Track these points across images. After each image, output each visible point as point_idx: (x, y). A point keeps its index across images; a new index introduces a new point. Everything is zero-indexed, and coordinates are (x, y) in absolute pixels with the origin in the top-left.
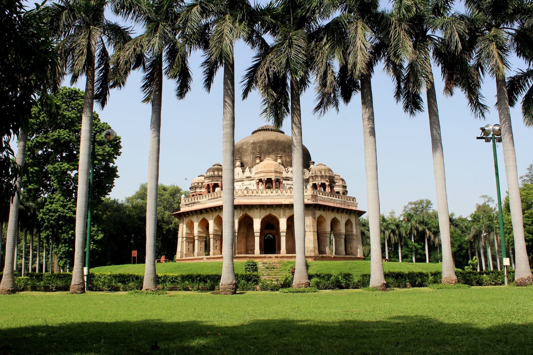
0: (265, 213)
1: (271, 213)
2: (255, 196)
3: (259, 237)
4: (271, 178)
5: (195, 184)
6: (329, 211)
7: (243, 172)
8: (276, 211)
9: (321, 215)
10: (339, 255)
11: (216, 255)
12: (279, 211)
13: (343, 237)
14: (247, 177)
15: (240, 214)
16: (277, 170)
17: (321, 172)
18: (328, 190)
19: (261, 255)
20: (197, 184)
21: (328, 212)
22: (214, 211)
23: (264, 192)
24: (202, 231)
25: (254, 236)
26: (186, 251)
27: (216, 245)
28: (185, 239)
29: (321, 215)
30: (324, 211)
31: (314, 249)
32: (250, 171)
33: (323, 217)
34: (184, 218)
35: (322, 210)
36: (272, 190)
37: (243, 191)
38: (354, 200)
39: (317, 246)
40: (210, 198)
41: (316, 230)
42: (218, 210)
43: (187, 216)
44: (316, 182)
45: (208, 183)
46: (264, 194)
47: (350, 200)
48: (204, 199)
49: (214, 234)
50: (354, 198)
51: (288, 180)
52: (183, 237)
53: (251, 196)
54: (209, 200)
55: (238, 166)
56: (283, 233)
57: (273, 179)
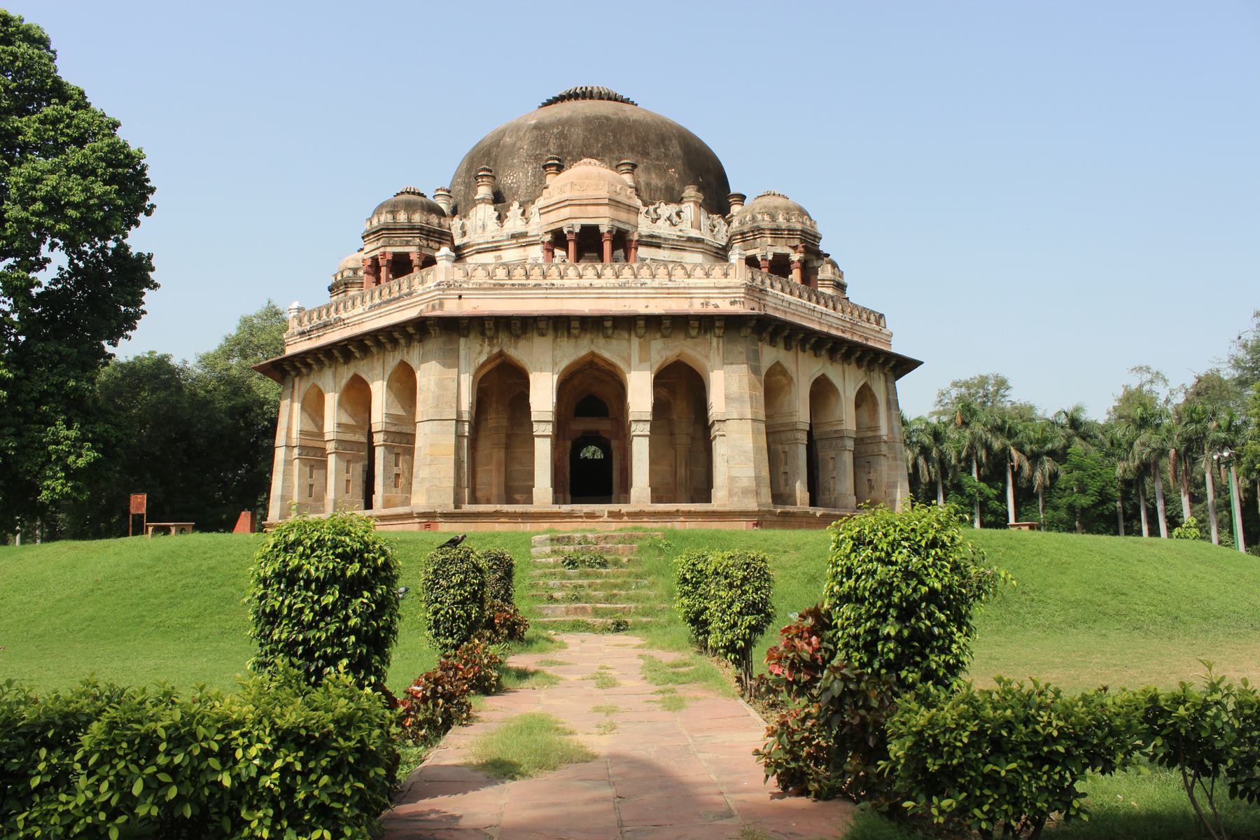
0: (572, 351)
1: (596, 351)
2: (537, 286)
3: (548, 441)
4: (596, 228)
5: (346, 274)
6: (804, 351)
7: (500, 218)
8: (614, 343)
9: (778, 363)
10: (835, 507)
11: (395, 506)
12: (625, 343)
13: (850, 444)
14: (513, 236)
15: (480, 353)
16: (619, 198)
17: (773, 218)
18: (795, 276)
19: (556, 508)
20: (351, 274)
21: (800, 354)
22: (388, 346)
23: (571, 272)
24: (351, 422)
25: (530, 439)
26: (300, 493)
27: (396, 470)
28: (296, 451)
29: (778, 363)
30: (788, 347)
31: (758, 485)
32: (523, 214)
33: (784, 372)
34: (297, 380)
35: (782, 345)
36: (599, 267)
37: (490, 268)
38: (882, 322)
39: (765, 472)
40: (377, 301)
41: (762, 414)
42: (402, 341)
43: (304, 370)
44: (758, 253)
45: (373, 254)
46: (569, 282)
47: (868, 320)
48: (359, 309)
49: (386, 432)
50: (881, 316)
51: (658, 246)
52: (289, 447)
53: (523, 286)
54: (372, 308)
55: (483, 200)
56: (641, 426)
57: (604, 229)
